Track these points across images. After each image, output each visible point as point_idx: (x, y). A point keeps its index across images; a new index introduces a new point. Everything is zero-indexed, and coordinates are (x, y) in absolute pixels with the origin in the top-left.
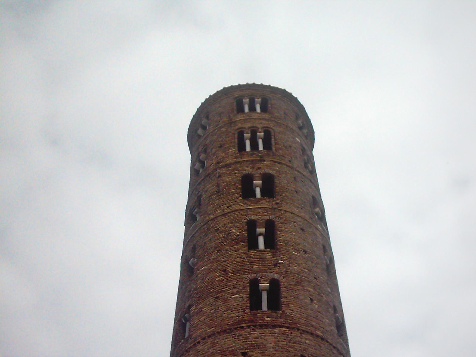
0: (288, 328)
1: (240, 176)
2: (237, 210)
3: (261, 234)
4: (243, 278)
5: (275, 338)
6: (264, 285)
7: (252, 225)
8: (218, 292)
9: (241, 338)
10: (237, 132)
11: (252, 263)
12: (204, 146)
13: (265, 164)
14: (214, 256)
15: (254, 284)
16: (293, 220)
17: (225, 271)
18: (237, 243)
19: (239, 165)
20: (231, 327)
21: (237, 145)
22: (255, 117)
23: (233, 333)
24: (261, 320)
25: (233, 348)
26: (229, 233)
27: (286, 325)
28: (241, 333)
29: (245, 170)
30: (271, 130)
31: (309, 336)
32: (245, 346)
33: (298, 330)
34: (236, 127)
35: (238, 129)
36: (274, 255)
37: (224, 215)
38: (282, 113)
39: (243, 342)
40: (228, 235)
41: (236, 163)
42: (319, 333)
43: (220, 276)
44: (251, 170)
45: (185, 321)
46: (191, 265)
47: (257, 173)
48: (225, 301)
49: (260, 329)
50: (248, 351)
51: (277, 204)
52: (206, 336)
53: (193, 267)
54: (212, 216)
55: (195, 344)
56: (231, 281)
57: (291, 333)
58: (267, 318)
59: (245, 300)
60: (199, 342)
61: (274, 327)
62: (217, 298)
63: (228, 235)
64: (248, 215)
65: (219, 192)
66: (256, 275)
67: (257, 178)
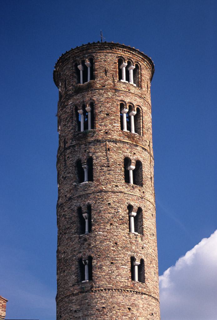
0: (147, 295)
1: (123, 158)
2: (121, 192)
3: (133, 216)
4: (127, 254)
5: (143, 302)
6: (138, 262)
7: (130, 208)
8: (112, 259)
9: (127, 298)
10: (119, 104)
11: (131, 243)
12: (91, 99)
13: (138, 150)
14: (108, 227)
15: (133, 259)
16: (150, 208)
17: (116, 243)
18: (123, 223)
19: (121, 145)
20: (122, 289)
21: (119, 120)
22: (133, 92)
23: (123, 293)
24: (137, 288)
25: (123, 303)
26: (117, 212)
27: (147, 293)
28: (128, 294)
29: (126, 153)
30: (140, 109)
31: (154, 300)
32: (130, 304)
33: (151, 296)
34: (119, 98)
35: (121, 101)
36: (142, 240)
37: (114, 192)
38: (146, 86)
39: (128, 301)
40: (117, 213)
41: (120, 141)
42: (157, 297)
43: (113, 247)
44: (130, 154)
45: (84, 263)
46: (84, 216)
47: (133, 158)
48: (118, 268)
49: (136, 294)
50: (131, 307)
51: (143, 192)
52: (107, 288)
53: (84, 218)
54: (104, 188)
55: (99, 290)
56: (120, 254)
57: (149, 299)
58: (140, 287)
59: (129, 271)
60: (102, 290)
61: (142, 294)
62: (112, 263)
63: (117, 213)
64: (129, 200)
65: (109, 166)
66: (133, 254)
67: (133, 164)
